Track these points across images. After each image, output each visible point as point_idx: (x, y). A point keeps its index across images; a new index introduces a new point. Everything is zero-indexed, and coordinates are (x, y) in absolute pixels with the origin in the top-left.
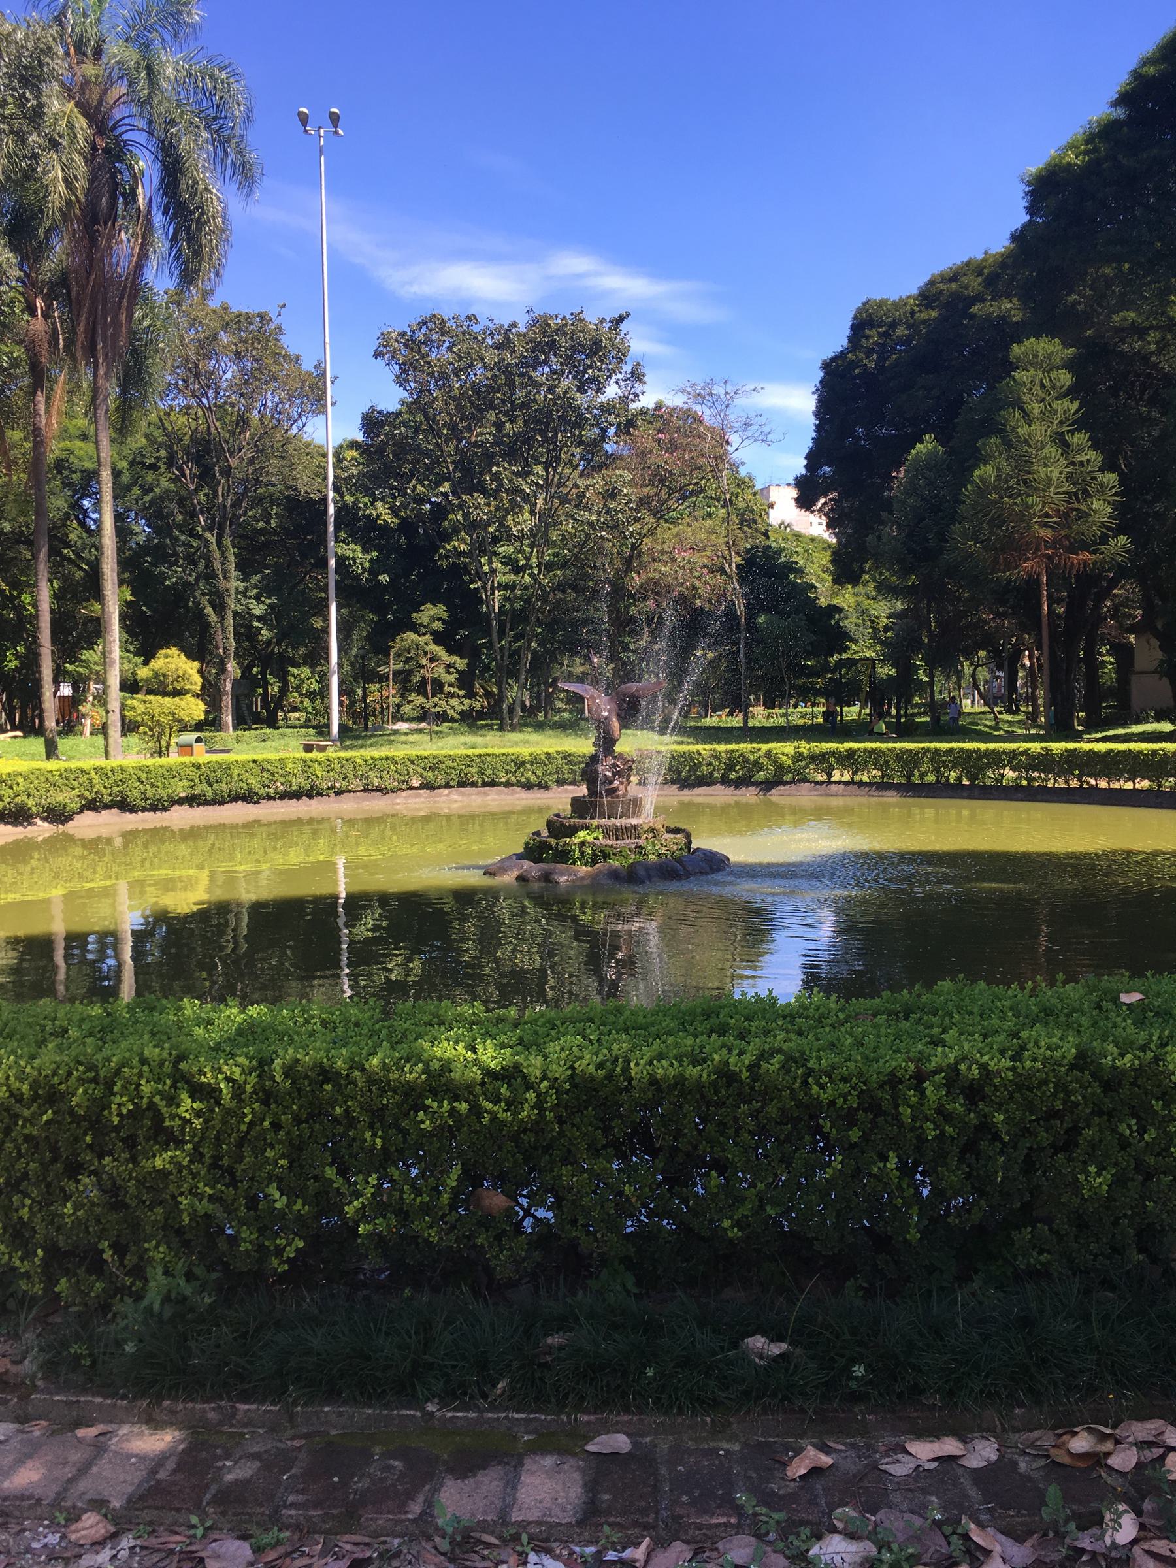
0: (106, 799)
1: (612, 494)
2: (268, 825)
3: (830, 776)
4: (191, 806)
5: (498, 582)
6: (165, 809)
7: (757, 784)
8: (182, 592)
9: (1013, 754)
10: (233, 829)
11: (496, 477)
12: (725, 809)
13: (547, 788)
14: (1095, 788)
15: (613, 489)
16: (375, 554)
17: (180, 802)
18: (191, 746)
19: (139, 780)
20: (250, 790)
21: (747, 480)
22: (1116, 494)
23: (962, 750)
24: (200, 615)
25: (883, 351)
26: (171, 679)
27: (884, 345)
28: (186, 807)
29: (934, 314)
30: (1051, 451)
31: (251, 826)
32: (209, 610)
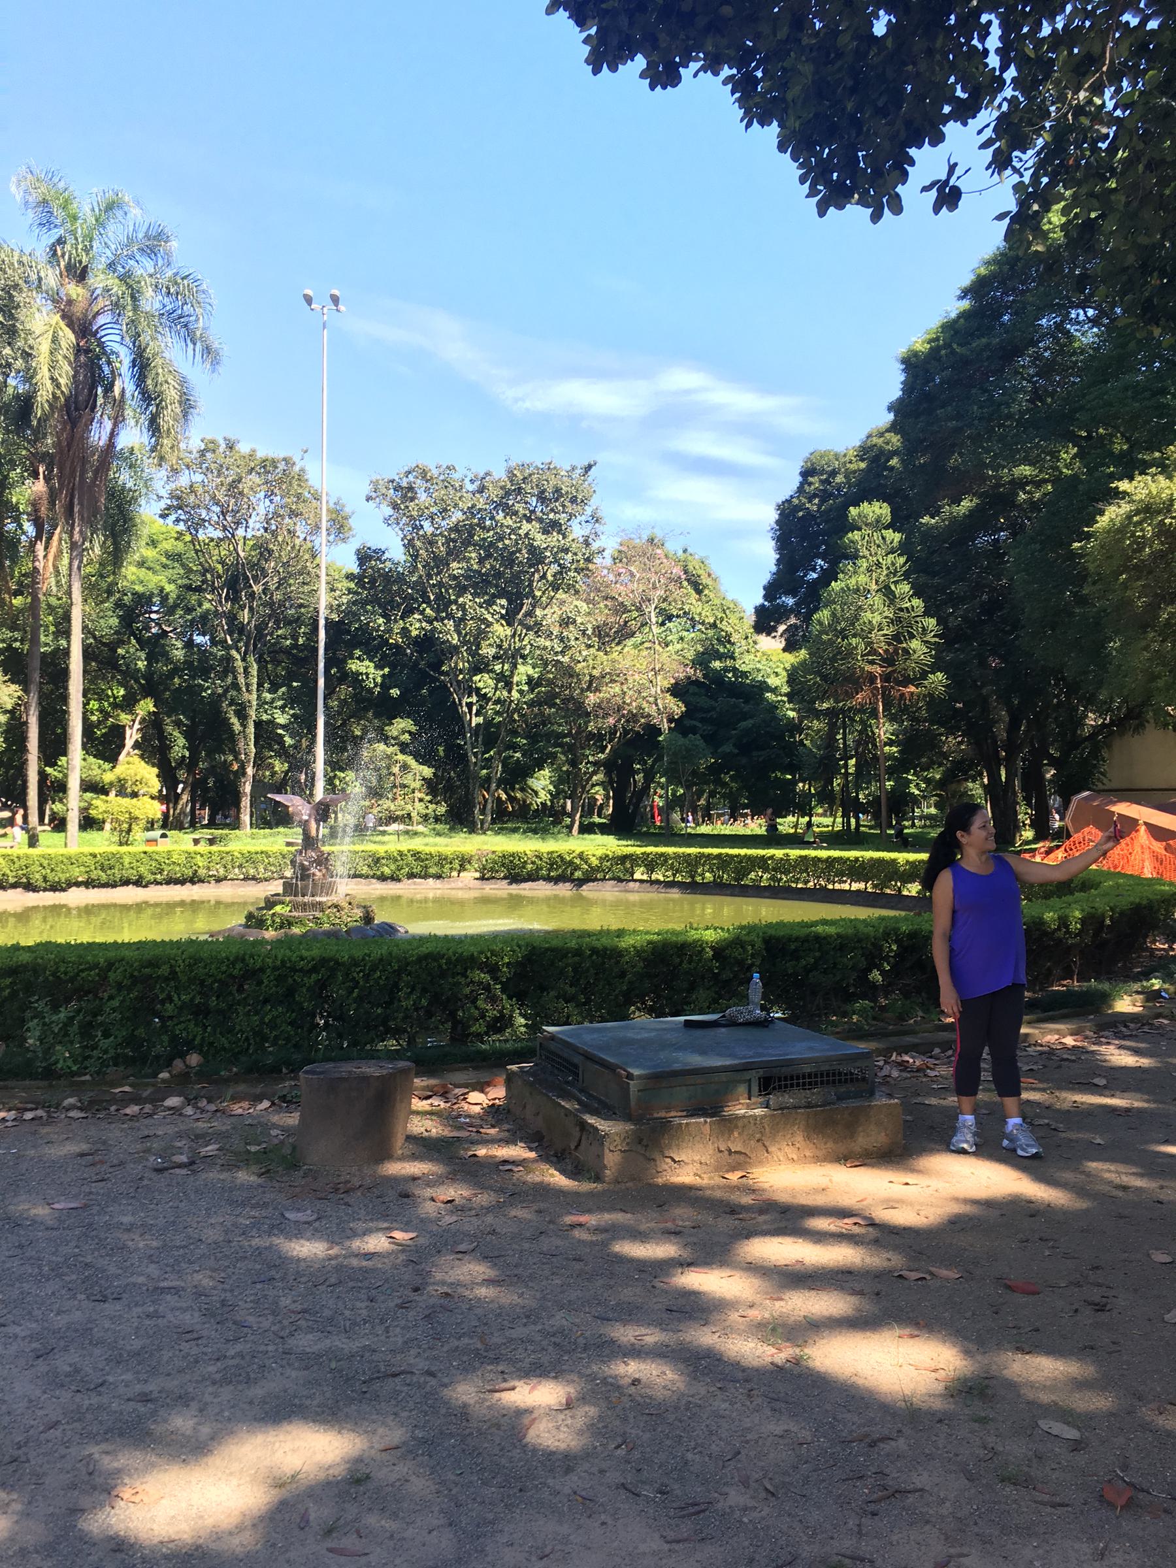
0: (12, 880)
1: (566, 622)
2: (157, 905)
3: (632, 874)
4: (87, 888)
5: (485, 697)
6: (64, 890)
7: (573, 881)
8: (216, 700)
9: (763, 859)
10: (125, 908)
11: (462, 607)
12: (547, 900)
13: (399, 880)
14: (824, 888)
15: (569, 618)
16: (387, 670)
17: (78, 884)
18: (156, 841)
19: (41, 865)
20: (141, 877)
21: (732, 606)
22: (934, 636)
23: (727, 855)
24: (230, 726)
25: (824, 496)
26: (130, 783)
27: (825, 491)
28: (82, 889)
29: (863, 465)
30: (877, 600)
31: (140, 907)
32: (234, 720)
